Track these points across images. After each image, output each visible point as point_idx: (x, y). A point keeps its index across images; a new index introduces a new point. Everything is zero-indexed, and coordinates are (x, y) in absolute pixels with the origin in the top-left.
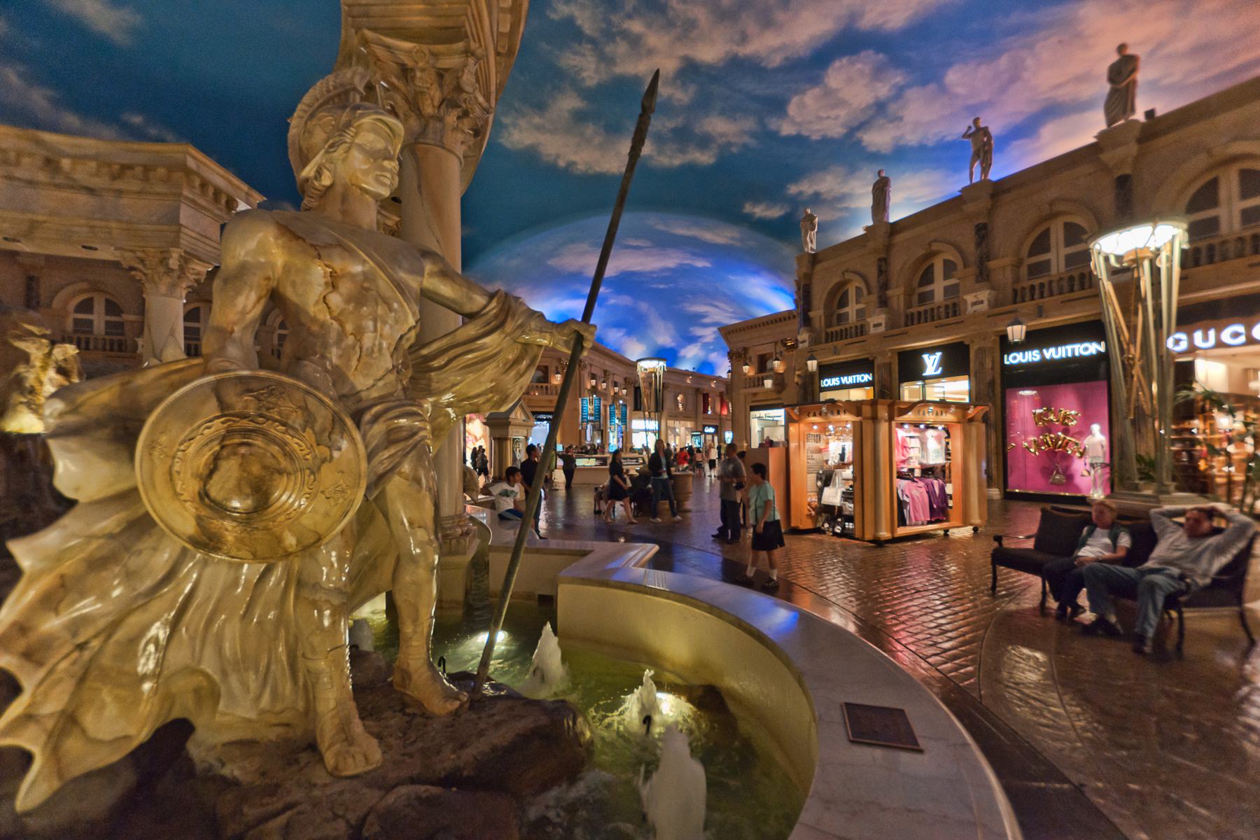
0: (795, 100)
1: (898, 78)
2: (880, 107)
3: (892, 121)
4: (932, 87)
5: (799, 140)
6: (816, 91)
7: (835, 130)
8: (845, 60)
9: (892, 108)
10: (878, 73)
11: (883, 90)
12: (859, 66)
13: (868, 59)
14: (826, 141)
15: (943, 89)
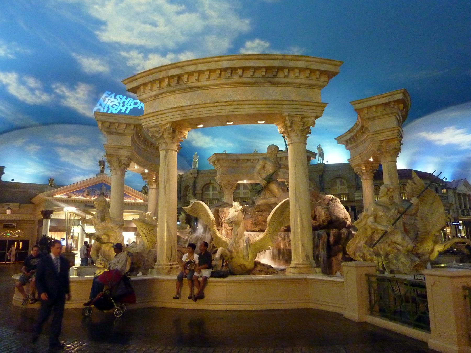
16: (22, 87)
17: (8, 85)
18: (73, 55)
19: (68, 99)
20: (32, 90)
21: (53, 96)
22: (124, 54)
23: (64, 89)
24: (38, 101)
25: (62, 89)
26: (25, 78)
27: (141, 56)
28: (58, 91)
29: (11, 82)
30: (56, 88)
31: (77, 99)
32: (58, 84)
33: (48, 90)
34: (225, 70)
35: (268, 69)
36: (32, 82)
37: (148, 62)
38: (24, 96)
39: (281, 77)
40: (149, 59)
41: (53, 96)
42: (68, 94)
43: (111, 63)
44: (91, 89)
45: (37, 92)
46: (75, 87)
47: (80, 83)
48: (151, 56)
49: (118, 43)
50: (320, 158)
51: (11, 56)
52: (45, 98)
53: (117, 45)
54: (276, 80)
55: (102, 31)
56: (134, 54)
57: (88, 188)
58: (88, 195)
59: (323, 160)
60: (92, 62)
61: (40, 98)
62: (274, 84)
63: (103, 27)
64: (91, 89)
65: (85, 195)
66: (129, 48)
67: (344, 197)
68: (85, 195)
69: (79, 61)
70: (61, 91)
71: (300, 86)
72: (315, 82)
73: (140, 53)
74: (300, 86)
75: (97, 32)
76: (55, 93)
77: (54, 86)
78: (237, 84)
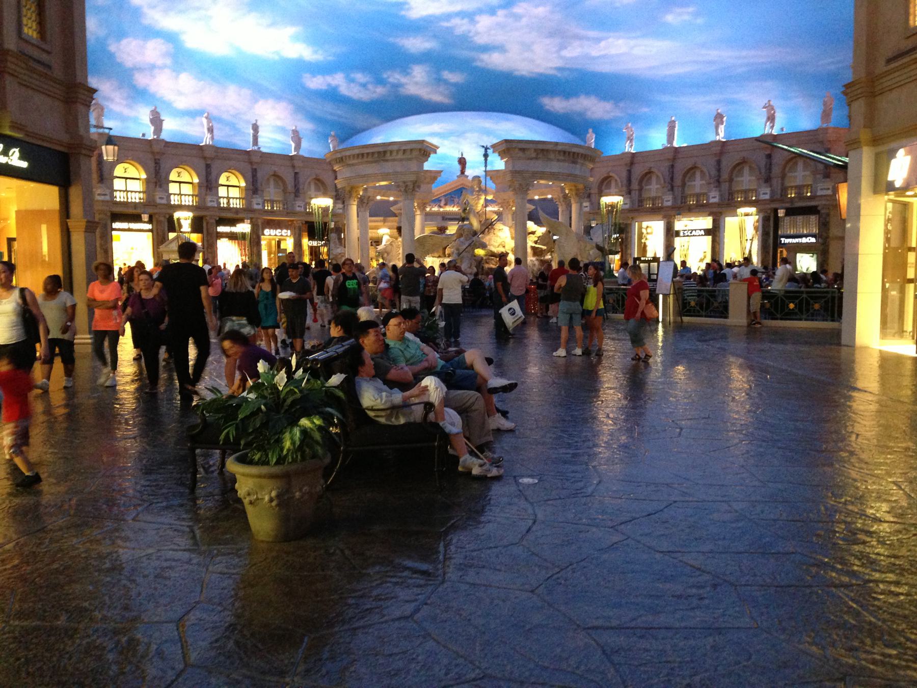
0: (130, 39)
1: (168, 61)
2: (153, 67)
3: (151, 76)
4: (174, 74)
5: (111, 56)
6: (141, 43)
7: (129, 62)
8: (163, 41)
9: (156, 71)
10: (166, 54)
11: (160, 62)
12: (164, 47)
13: (170, 47)
14: (120, 65)
15: (177, 77)
16: (352, 85)
17: (337, 87)
18: (391, 40)
19: (407, 87)
20: (364, 86)
21: (388, 85)
22: (446, 24)
23: (397, 76)
24: (375, 96)
25: (395, 77)
26: (352, 75)
27: (466, 21)
28: (391, 80)
29: (340, 83)
30: (388, 77)
31: (416, 83)
32: (389, 73)
33: (380, 82)
34: (358, 155)
35: (379, 153)
36: (360, 77)
37: (478, 26)
38: (358, 94)
39: (388, 156)
40: (478, 22)
41: (388, 85)
42: (403, 80)
43: (435, 36)
44: (428, 69)
45: (370, 87)
46: (409, 71)
47: (411, 65)
48: (477, 18)
49: (431, 16)
50: (768, 123)
51: (330, 58)
52: (380, 91)
53: (432, 19)
54: (386, 158)
55: (408, 9)
56: (456, 21)
57: (445, 196)
58: (446, 204)
59: (772, 127)
60: (414, 41)
61: (375, 92)
62: (387, 161)
63: (407, 6)
64: (428, 69)
65: (442, 204)
66: (448, 17)
67: (754, 194)
68: (442, 204)
69: (401, 44)
70: (395, 79)
71: (401, 160)
72: (410, 157)
73: (463, 19)
74: (401, 160)
75: (403, 13)
76: (390, 83)
77: (385, 76)
78: (368, 162)
